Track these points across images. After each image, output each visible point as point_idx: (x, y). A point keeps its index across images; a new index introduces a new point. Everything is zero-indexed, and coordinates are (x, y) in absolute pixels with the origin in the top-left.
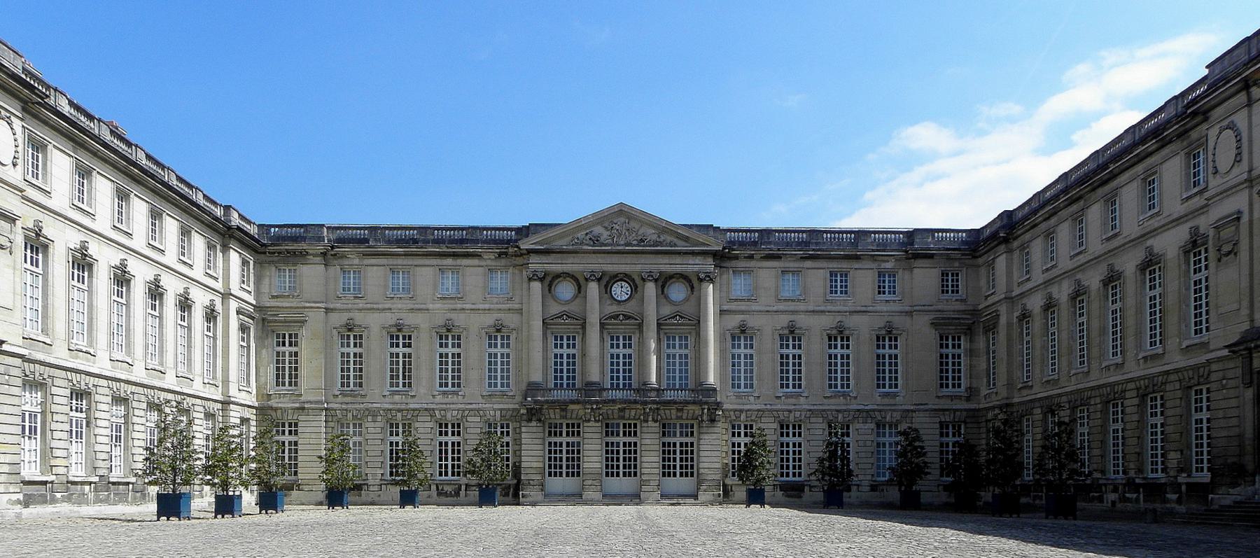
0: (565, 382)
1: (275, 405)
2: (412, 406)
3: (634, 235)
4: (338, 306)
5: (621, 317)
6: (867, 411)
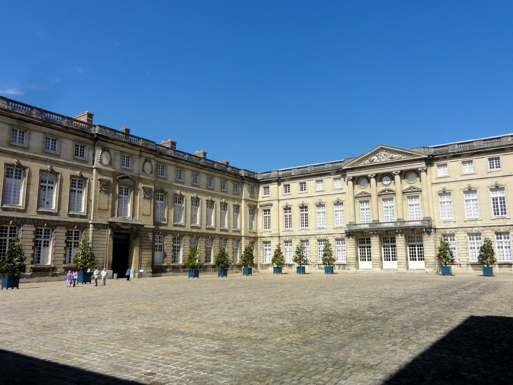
1: (264, 236)
5: (387, 191)
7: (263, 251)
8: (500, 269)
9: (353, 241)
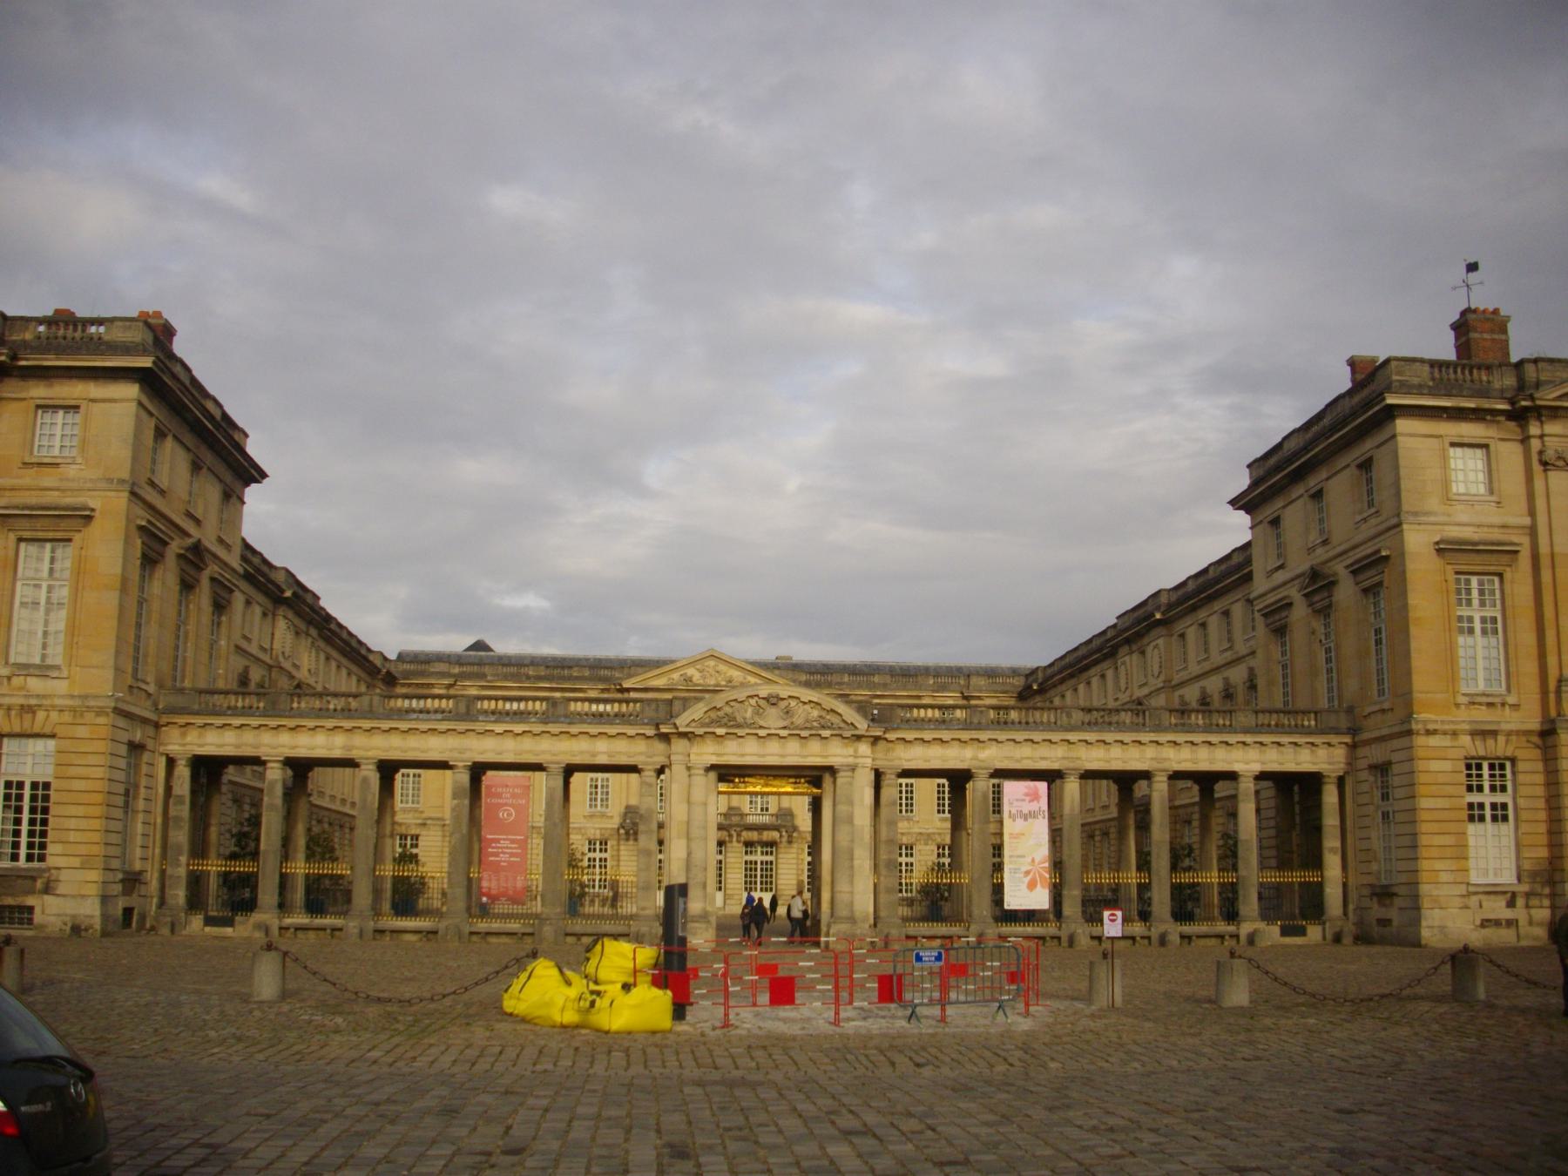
1: (400, 821)
6: (929, 835)
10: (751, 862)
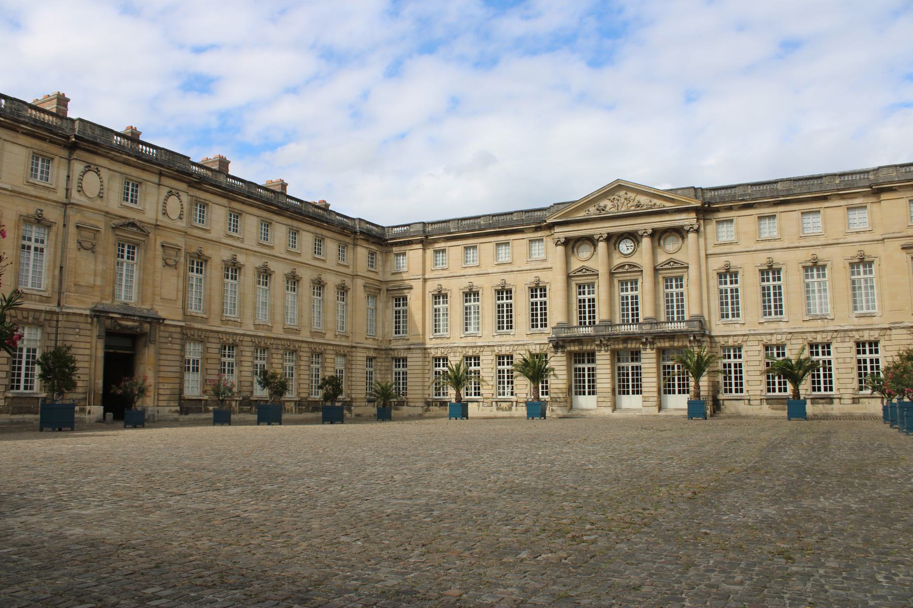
0: (587, 321)
1: (393, 347)
2: (478, 344)
3: (631, 203)
4: (432, 276)
5: (627, 267)
7: (392, 376)
8: (815, 408)
9: (564, 358)
10: (669, 367)
